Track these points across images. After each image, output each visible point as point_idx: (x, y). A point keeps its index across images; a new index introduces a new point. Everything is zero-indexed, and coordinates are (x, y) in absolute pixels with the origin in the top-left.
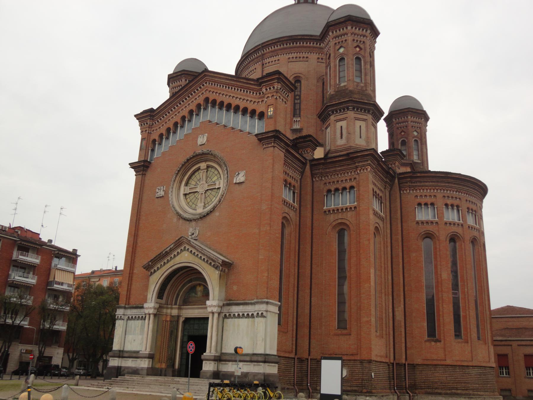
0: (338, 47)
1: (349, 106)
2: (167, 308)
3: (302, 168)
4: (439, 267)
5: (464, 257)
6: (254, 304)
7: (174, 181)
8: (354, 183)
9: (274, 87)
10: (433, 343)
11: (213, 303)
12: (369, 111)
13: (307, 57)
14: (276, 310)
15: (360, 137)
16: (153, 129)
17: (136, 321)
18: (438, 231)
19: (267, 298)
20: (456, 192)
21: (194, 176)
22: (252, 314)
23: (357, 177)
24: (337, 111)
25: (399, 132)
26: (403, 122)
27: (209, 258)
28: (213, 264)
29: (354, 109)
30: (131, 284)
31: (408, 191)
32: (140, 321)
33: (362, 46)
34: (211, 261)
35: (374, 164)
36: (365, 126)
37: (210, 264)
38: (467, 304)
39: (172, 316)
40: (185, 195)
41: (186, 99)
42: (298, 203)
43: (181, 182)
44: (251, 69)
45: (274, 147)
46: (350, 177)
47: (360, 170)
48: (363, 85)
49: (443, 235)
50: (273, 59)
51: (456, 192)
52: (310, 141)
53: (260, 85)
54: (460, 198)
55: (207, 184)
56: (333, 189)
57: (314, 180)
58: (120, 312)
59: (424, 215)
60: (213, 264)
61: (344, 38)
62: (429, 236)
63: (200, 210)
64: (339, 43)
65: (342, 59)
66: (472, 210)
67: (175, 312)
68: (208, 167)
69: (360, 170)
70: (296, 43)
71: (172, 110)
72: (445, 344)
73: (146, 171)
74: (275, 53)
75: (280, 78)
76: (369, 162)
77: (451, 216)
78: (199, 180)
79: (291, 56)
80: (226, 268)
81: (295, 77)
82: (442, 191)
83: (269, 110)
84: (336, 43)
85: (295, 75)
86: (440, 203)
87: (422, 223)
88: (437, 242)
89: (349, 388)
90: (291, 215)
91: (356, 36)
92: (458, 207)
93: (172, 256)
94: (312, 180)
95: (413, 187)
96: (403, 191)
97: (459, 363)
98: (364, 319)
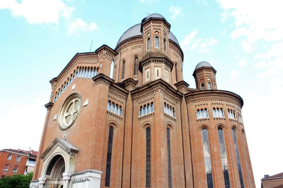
0: (147, 34)
1: (151, 60)
2: (52, 180)
3: (126, 97)
4: (212, 145)
5: (228, 138)
6: (84, 173)
7: (61, 110)
8: (153, 100)
9: (103, 53)
12: (162, 62)
14: (99, 176)
15: (158, 76)
18: (210, 124)
19: (91, 169)
20: (219, 100)
23: (154, 96)
25: (200, 80)
26: (201, 75)
27: (66, 148)
29: (153, 61)
30: (39, 168)
31: (191, 103)
33: (159, 31)
35: (164, 88)
36: (160, 70)
38: (232, 167)
39: (54, 185)
40: (66, 117)
42: (124, 115)
45: (101, 83)
46: (151, 97)
48: (159, 49)
49: (213, 126)
50: (125, 49)
51: (219, 100)
52: (130, 81)
53: (97, 54)
54: (222, 104)
57: (134, 102)
59: (202, 116)
61: (149, 29)
62: (205, 127)
65: (149, 39)
66: (231, 110)
67: (56, 182)
68: (76, 101)
69: (155, 92)
70: (135, 40)
73: (51, 108)
74: (126, 46)
75: (105, 48)
76: (160, 87)
77: (218, 114)
78: (72, 109)
79: (133, 46)
81: (135, 56)
82: (211, 101)
84: (146, 32)
86: (210, 107)
87: (200, 120)
90: (118, 122)
91: (155, 27)
92: (221, 109)
93: (53, 150)
94: (133, 102)
95: (194, 100)
98: (158, 180)
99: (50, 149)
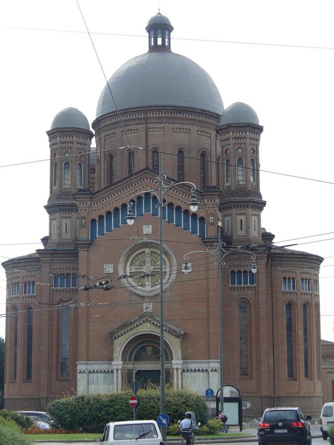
9: (214, 201)
10: (292, 382)
11: (177, 363)
13: (189, 129)
14: (216, 365)
16: (91, 209)
17: (98, 374)
21: (137, 258)
22: (206, 370)
24: (238, 207)
28: (174, 334)
32: (103, 374)
33: (255, 149)
34: (172, 332)
37: (172, 334)
41: (126, 189)
43: (126, 262)
44: (132, 127)
47: (259, 260)
48: (255, 184)
53: (204, 195)
55: (152, 267)
56: (236, 271)
58: (81, 367)
60: (174, 334)
63: (148, 288)
64: (238, 144)
68: (152, 252)
69: (259, 260)
70: (180, 114)
71: (112, 196)
72: (299, 382)
74: (161, 120)
79: (175, 126)
80: (184, 337)
83: (210, 218)
85: (179, 147)
88: (296, 308)
89: (252, 415)
96: (274, 267)
97: (307, 395)
99: (131, 323)
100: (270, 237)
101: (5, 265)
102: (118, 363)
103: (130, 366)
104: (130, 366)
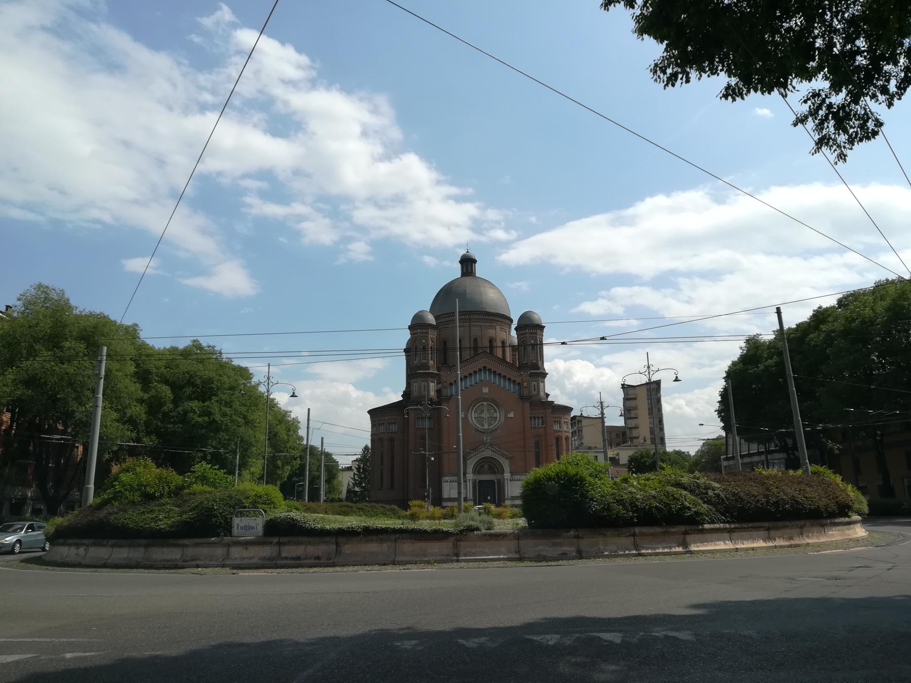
11: (507, 475)
63: (486, 427)
80: (510, 459)
100: (548, 395)
101: (370, 412)
102: (470, 476)
103: (476, 477)
104: (476, 477)
